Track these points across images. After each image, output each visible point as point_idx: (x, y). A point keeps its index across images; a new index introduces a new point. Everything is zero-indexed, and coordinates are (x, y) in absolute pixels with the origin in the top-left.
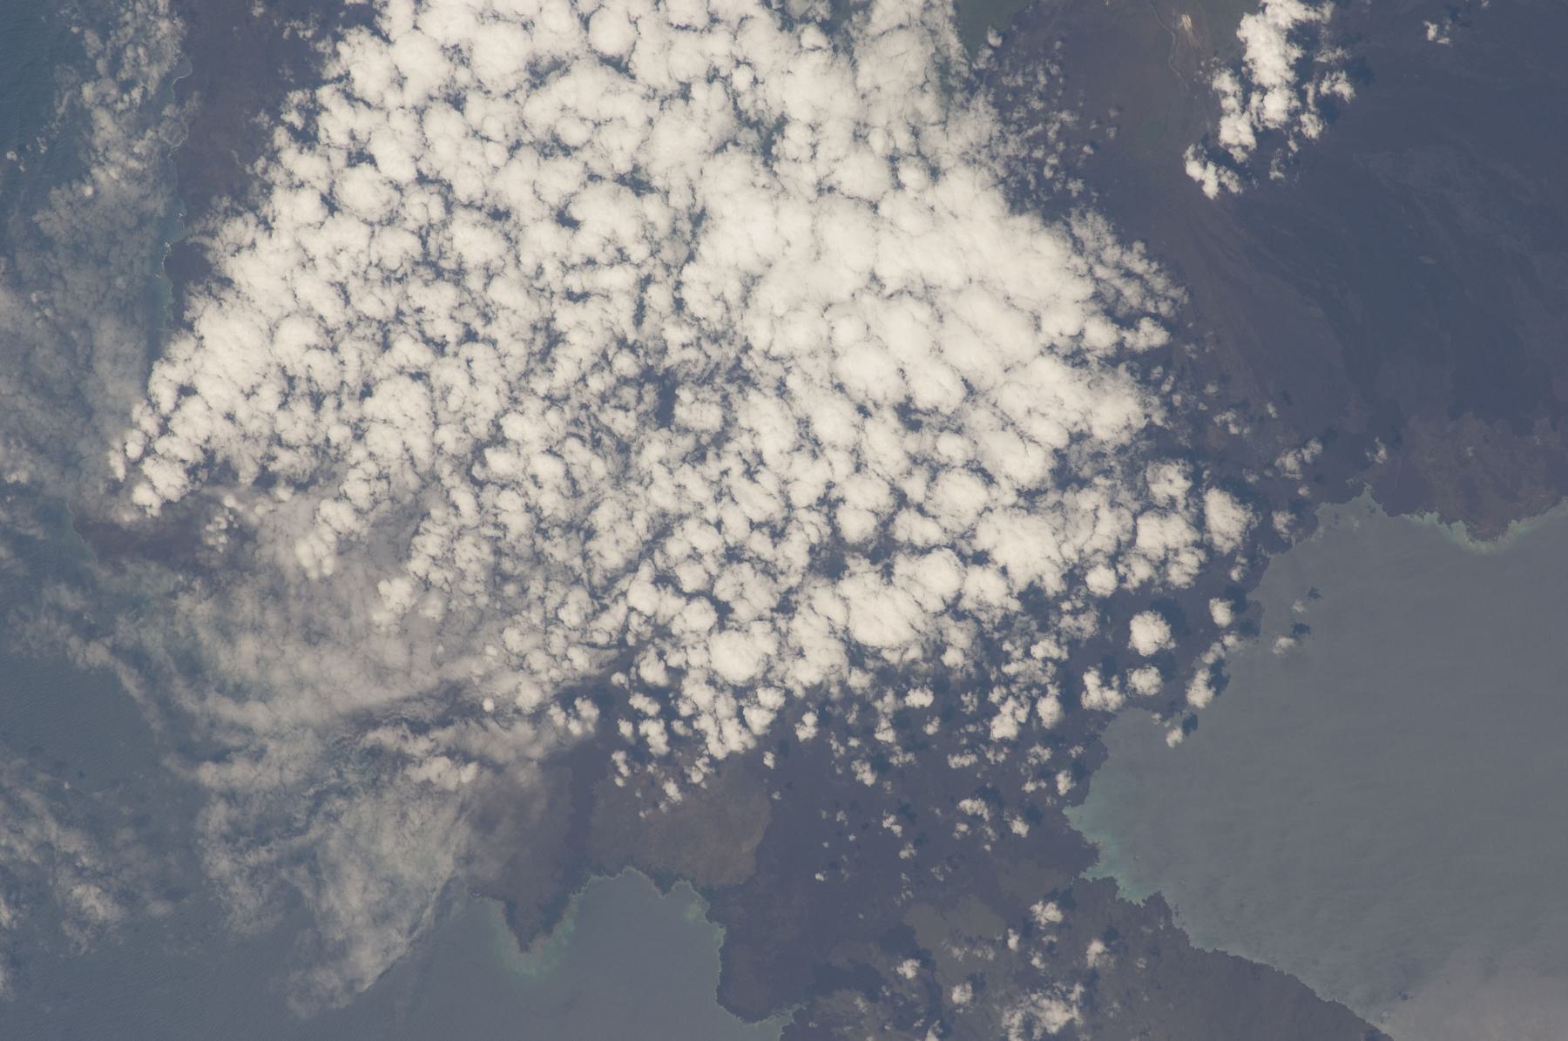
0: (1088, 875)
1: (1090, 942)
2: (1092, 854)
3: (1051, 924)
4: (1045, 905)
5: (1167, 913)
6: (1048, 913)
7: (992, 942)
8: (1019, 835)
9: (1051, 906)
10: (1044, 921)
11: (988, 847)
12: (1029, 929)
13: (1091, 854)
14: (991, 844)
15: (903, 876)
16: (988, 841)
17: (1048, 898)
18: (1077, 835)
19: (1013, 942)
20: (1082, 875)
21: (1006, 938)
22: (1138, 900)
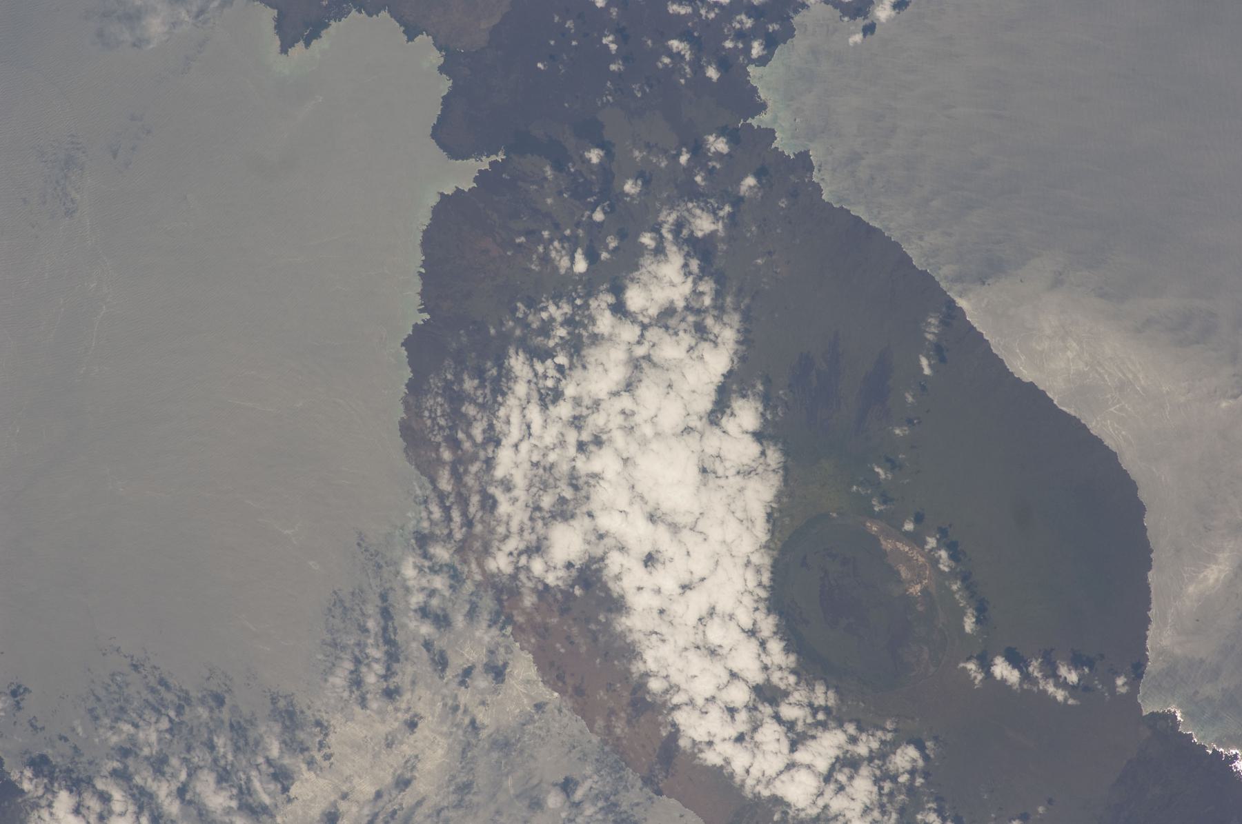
0: (754, 122)
1: (746, 176)
2: (762, 107)
3: (719, 156)
4: (717, 137)
5: (810, 168)
6: (719, 145)
7: (665, 152)
8: (710, 78)
9: (722, 139)
10: (713, 149)
11: (683, 81)
12: (698, 149)
13: (762, 107)
14: (686, 79)
15: (609, 84)
16: (684, 76)
17: (722, 132)
18: (755, 90)
19: (684, 159)
20: (749, 121)
21: (679, 154)
22: (790, 152)
